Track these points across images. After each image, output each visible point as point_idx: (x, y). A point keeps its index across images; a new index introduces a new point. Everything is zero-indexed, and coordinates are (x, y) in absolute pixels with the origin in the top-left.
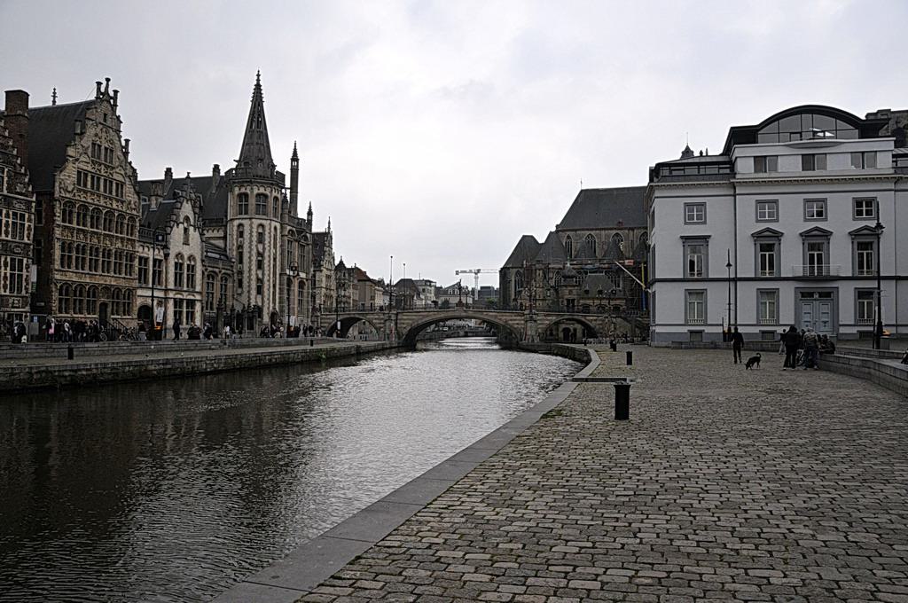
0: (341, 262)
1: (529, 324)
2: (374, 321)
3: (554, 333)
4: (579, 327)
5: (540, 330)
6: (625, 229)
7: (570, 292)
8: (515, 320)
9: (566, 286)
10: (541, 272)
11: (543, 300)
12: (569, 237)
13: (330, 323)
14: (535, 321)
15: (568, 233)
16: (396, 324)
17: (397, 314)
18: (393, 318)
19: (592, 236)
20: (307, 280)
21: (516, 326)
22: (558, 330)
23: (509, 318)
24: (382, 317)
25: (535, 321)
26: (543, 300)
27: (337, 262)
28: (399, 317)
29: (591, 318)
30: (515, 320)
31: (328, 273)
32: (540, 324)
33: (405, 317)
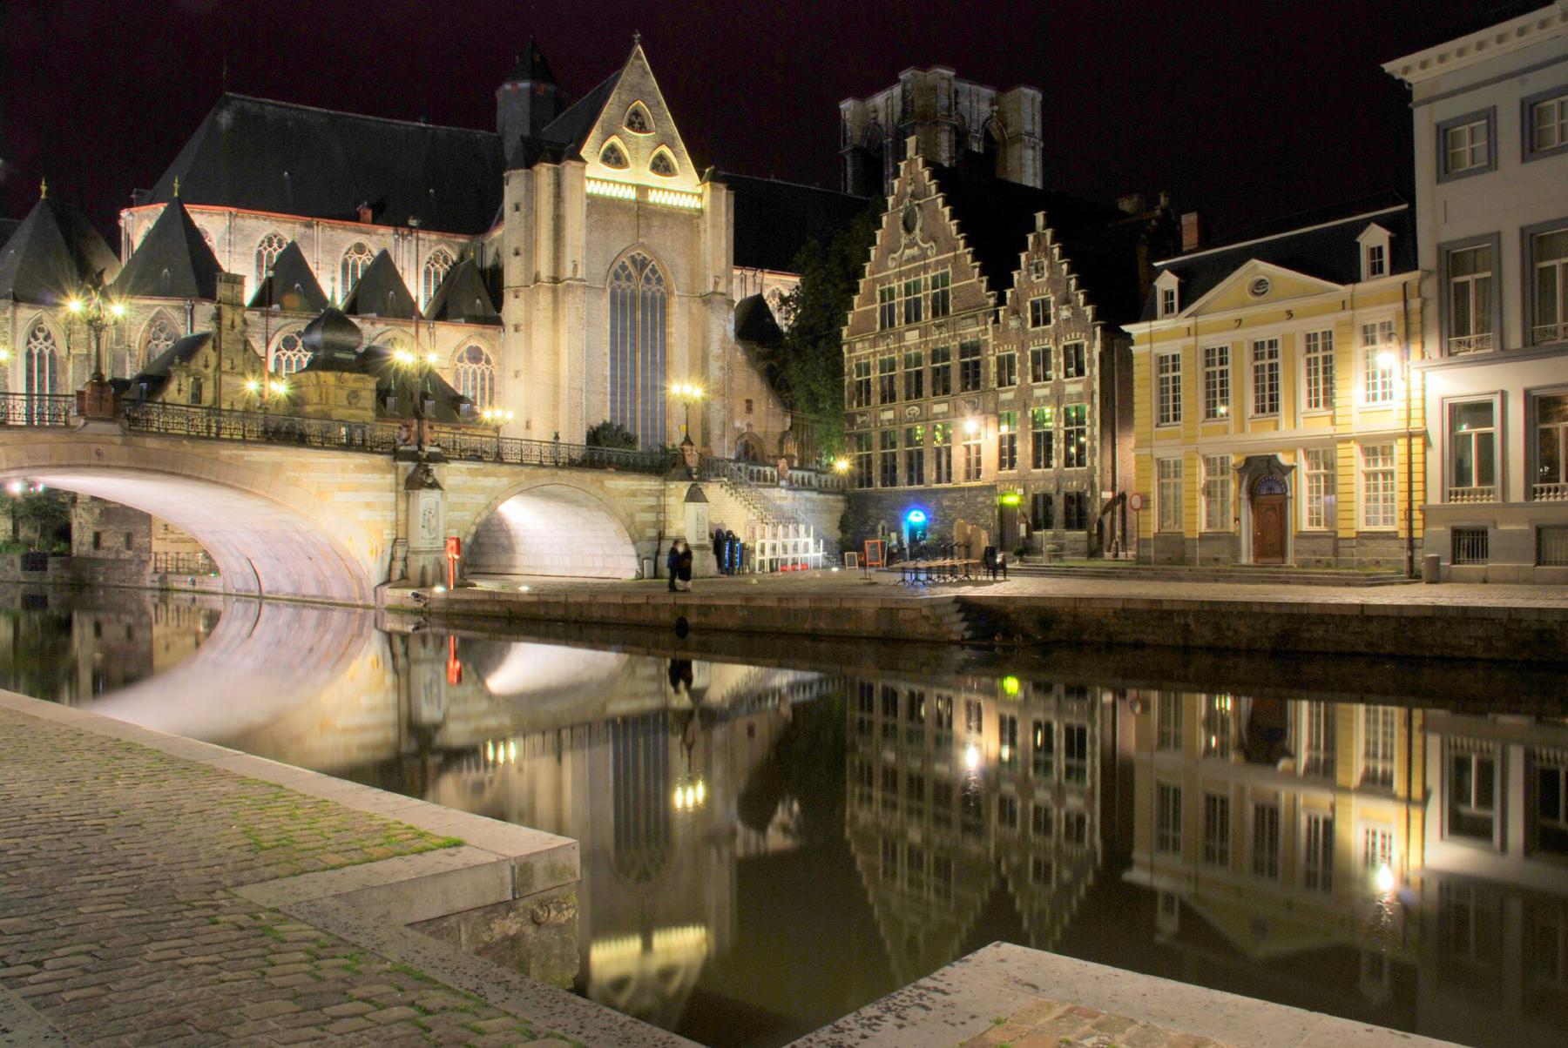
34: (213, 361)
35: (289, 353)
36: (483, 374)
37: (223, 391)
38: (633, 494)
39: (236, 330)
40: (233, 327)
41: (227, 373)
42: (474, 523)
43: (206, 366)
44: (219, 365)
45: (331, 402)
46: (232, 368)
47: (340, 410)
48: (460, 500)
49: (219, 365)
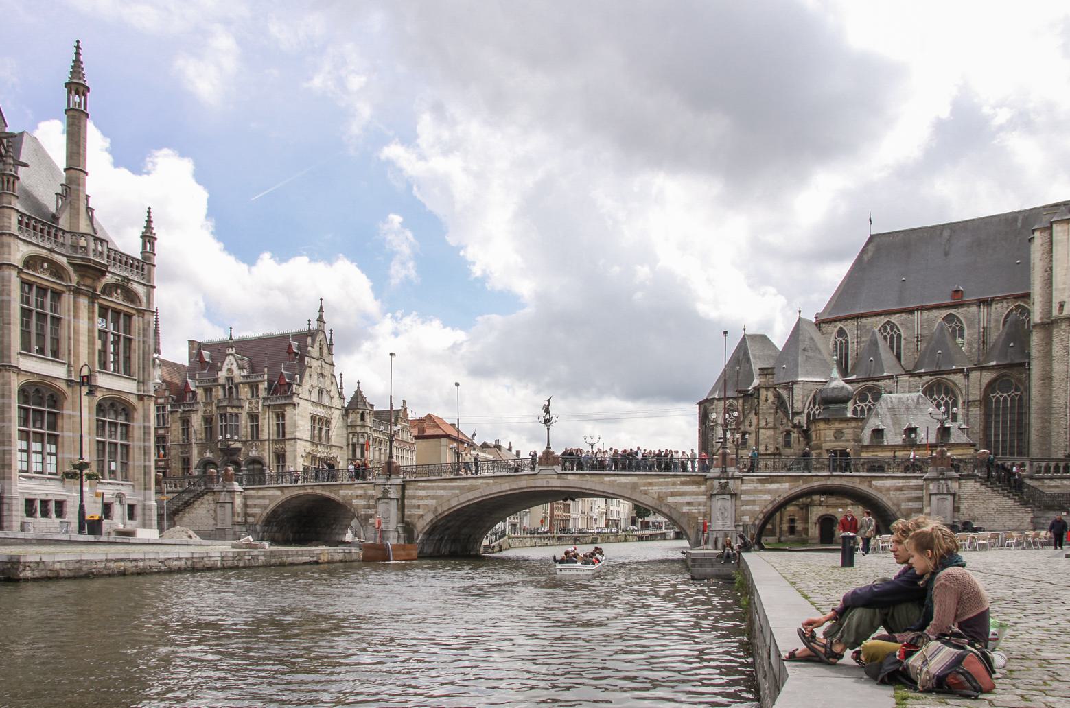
0: (358, 393)
1: (718, 503)
2: (355, 502)
3: (799, 526)
4: (856, 511)
5: (746, 519)
6: (970, 304)
7: (839, 434)
8: (682, 494)
9: (827, 421)
10: (770, 394)
11: (774, 454)
12: (841, 333)
13: (265, 507)
14: (734, 495)
15: (839, 325)
16: (402, 508)
17: (403, 486)
18: (394, 494)
19: (893, 326)
20: (141, 398)
21: (685, 509)
22: (806, 520)
23: (664, 489)
24: (371, 492)
25: (734, 495)
26: (774, 454)
27: (349, 393)
28: (408, 492)
29: (888, 483)
30: (682, 494)
31: (320, 412)
32: (747, 503)
33: (422, 493)
34: (754, 421)
35: (863, 405)
36: (1012, 400)
37: (760, 439)
38: (900, 489)
39: (769, 401)
40: (767, 400)
41: (763, 428)
42: (762, 512)
43: (750, 426)
44: (758, 425)
45: (822, 439)
46: (766, 425)
47: (828, 444)
48: (751, 499)
49: (758, 425)
